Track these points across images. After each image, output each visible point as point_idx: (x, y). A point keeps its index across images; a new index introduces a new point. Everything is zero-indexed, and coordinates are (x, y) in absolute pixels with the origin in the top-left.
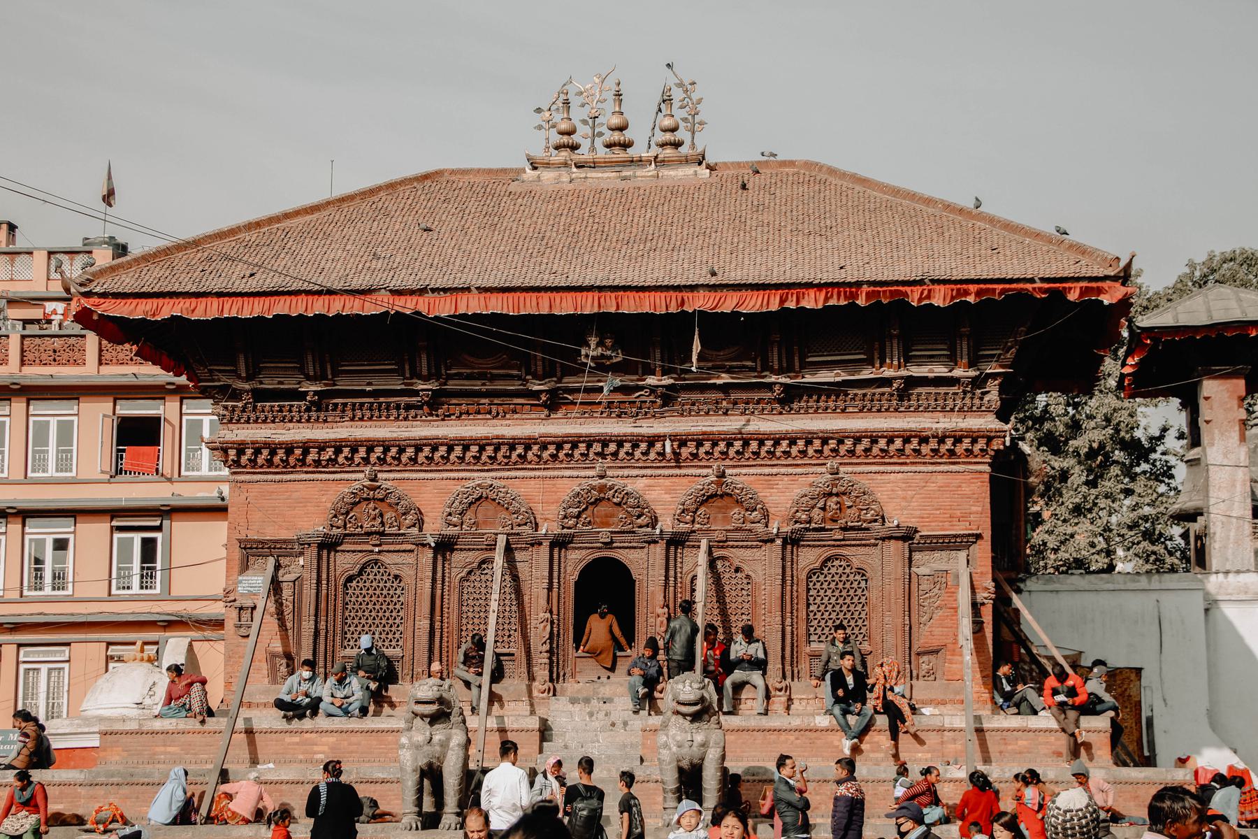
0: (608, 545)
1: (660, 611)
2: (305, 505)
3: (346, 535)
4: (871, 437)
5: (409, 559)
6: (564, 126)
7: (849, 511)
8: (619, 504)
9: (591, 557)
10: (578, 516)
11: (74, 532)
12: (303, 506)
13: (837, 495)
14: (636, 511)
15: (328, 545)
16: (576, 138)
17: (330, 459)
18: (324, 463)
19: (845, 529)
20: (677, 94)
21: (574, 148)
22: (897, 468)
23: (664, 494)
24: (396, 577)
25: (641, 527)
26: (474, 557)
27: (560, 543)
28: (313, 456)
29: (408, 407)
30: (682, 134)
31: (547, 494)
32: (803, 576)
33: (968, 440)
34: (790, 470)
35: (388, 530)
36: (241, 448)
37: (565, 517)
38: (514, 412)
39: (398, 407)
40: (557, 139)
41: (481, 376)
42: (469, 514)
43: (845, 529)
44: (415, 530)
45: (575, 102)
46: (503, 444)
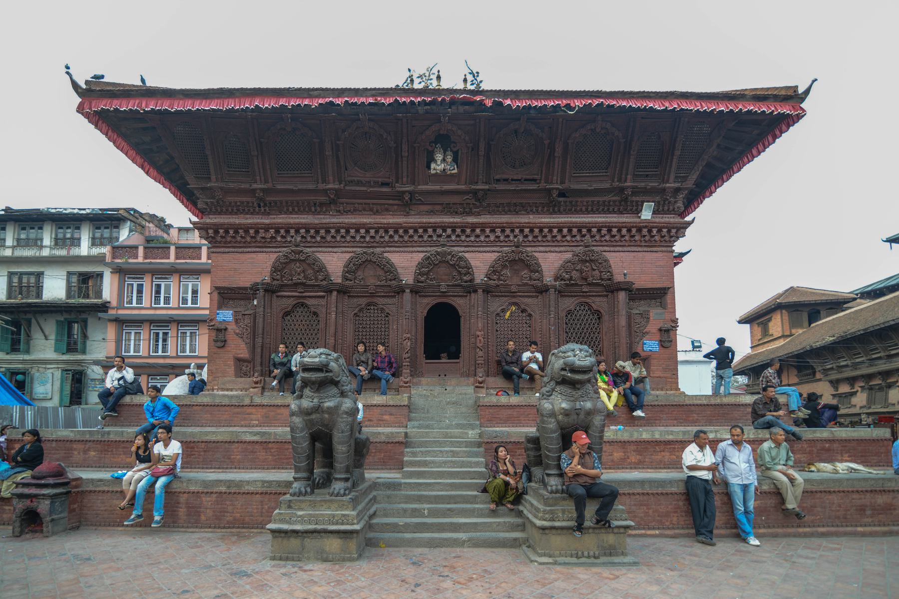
1: (479, 333)
2: (255, 267)
3: (282, 286)
4: (609, 227)
5: (323, 302)
7: (594, 273)
8: (453, 266)
9: (435, 302)
10: (427, 274)
13: (587, 261)
15: (270, 290)
17: (272, 237)
19: (589, 284)
22: (621, 249)
23: (481, 262)
25: (466, 282)
26: (363, 301)
27: (415, 291)
28: (262, 233)
32: (564, 314)
34: (557, 249)
35: (309, 283)
36: (216, 228)
37: (419, 274)
38: (387, 210)
42: (360, 273)
43: (589, 284)
44: (324, 283)
46: (381, 228)
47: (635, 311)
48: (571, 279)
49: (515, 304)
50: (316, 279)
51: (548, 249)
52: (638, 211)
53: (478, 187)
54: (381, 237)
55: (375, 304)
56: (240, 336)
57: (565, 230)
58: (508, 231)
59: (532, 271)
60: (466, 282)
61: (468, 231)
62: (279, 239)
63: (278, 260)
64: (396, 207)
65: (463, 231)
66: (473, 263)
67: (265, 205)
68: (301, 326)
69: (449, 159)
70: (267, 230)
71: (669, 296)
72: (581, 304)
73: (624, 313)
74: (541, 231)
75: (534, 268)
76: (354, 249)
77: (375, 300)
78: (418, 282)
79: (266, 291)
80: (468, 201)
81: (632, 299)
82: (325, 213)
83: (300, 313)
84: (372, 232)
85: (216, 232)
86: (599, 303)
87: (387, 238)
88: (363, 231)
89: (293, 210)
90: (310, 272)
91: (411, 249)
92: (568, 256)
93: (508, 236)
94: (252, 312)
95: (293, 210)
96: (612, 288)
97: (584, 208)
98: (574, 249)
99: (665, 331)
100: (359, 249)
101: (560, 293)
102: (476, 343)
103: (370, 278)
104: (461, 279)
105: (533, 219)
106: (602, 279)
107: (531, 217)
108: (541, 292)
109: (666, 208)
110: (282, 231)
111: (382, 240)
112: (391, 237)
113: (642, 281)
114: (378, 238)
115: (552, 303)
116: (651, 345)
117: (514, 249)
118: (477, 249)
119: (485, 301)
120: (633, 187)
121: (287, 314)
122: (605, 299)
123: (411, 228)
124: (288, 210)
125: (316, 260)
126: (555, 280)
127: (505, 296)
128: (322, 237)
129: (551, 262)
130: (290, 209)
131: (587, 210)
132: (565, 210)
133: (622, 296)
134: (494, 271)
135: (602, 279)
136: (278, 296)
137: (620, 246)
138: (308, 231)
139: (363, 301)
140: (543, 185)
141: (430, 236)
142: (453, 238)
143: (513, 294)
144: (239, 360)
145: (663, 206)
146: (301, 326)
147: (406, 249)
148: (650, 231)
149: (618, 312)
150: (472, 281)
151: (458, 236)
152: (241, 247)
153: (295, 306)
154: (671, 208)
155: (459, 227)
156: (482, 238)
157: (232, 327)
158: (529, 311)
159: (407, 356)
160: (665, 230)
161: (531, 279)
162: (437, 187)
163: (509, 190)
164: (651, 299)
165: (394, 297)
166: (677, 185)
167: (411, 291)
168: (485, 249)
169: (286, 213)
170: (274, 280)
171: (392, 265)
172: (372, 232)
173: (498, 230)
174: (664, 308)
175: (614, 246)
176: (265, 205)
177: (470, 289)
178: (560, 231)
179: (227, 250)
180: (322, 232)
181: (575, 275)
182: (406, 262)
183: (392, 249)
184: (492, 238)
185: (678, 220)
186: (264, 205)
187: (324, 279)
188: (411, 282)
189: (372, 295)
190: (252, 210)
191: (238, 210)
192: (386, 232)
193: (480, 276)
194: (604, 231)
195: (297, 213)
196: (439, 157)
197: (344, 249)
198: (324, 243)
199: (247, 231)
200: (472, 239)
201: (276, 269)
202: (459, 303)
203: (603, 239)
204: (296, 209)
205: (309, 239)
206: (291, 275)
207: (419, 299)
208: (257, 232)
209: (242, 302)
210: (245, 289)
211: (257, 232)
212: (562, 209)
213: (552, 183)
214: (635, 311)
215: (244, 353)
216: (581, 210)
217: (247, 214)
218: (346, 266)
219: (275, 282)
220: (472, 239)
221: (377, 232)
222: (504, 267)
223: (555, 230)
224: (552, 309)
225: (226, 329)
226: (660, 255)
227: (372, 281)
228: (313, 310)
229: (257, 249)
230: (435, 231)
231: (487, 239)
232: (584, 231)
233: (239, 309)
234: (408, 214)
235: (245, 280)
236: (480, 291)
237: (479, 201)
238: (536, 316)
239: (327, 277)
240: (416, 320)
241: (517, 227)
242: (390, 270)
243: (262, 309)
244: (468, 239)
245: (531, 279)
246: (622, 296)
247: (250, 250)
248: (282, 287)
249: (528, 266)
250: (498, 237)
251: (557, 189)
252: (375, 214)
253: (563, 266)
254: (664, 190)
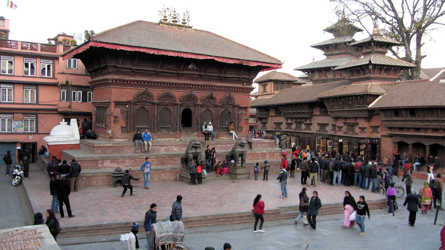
0: (188, 106)
6: (165, 16)
11: (14, 88)
16: (167, 18)
20: (186, 13)
21: (166, 20)
24: (147, 111)
29: (153, 74)
30: (186, 21)
31: (178, 94)
39: (145, 74)
40: (164, 18)
41: (170, 69)
45: (167, 11)
66: (198, 96)
81: (239, 109)
86: (230, 110)
90: (148, 97)
96: (234, 106)
144: (122, 127)
189: (166, 105)
202: (192, 109)
215: (124, 125)
222: (206, 99)
235: (123, 99)
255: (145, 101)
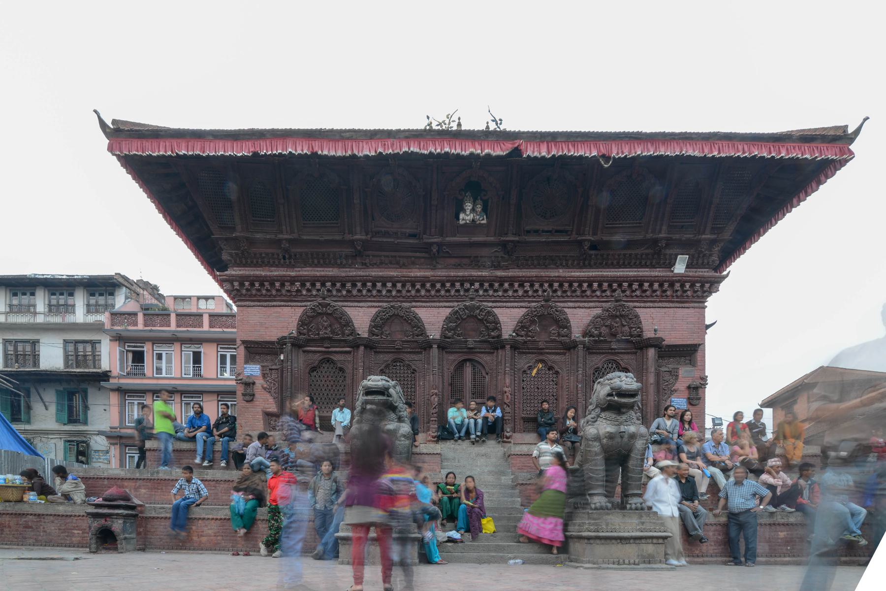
1: (506, 389)
7: (624, 329)
10: (454, 329)
12: (280, 321)
14: (491, 326)
17: (298, 291)
18: (294, 294)
19: (618, 341)
25: (493, 338)
33: (698, 285)
34: (586, 305)
35: (336, 337)
37: (447, 329)
38: (413, 263)
42: (386, 328)
44: (351, 338)
46: (409, 281)
47: (663, 369)
48: (600, 335)
49: (542, 361)
50: (343, 334)
51: (577, 305)
52: (671, 264)
53: (508, 239)
54: (408, 291)
55: (402, 361)
56: (268, 390)
57: (595, 285)
58: (537, 286)
59: (560, 327)
60: (493, 338)
61: (496, 285)
62: (304, 292)
63: (304, 313)
64: (422, 260)
65: (491, 286)
66: (502, 319)
67: (290, 258)
68: (328, 383)
69: (479, 208)
70: (292, 283)
71: (699, 354)
72: (609, 361)
73: (653, 370)
74: (571, 286)
75: (563, 324)
76: (380, 304)
77: (401, 356)
78: (446, 337)
79: (293, 345)
80: (497, 254)
82: (350, 266)
83: (326, 369)
84: (399, 285)
85: (242, 285)
87: (413, 293)
88: (389, 285)
89: (319, 262)
91: (438, 304)
92: (598, 311)
93: (537, 291)
94: (278, 367)
95: (319, 262)
97: (615, 262)
98: (604, 304)
99: (694, 388)
100: (385, 304)
101: (590, 350)
102: (503, 399)
103: (397, 333)
104: (489, 335)
105: (561, 272)
106: (631, 336)
107: (561, 271)
108: (569, 349)
109: (700, 261)
110: (308, 284)
111: (409, 294)
112: (418, 291)
113: (672, 338)
114: (404, 292)
115: (581, 359)
116: (679, 402)
117: (543, 303)
118: (505, 304)
119: (513, 358)
120: (667, 239)
121: (313, 369)
122: (633, 357)
123: (438, 281)
124: (313, 262)
125: (343, 314)
126: (583, 337)
127: (533, 353)
128: (349, 291)
129: (580, 318)
130: (316, 261)
131: (618, 263)
132: (595, 264)
133: (651, 352)
134: (522, 326)
135: (631, 336)
136: (304, 352)
137: (651, 302)
138: (334, 285)
139: (389, 357)
140: (574, 236)
141: (458, 291)
142: (481, 292)
143: (540, 351)
145: (697, 260)
146: (328, 383)
147: (433, 304)
148: (682, 286)
149: (647, 369)
150: (500, 336)
151: (486, 291)
152: (266, 301)
153: (321, 362)
154: (706, 261)
155: (487, 281)
156: (510, 293)
157: (260, 382)
158: (556, 368)
159: (434, 411)
160: (698, 285)
161: (559, 335)
162: (466, 239)
163: (540, 242)
164: (680, 357)
165: (421, 353)
166: (713, 237)
167: (438, 347)
168: (512, 304)
169: (311, 266)
170: (301, 334)
171: (419, 320)
172: (399, 285)
173: (527, 285)
174: (694, 366)
175: (645, 302)
176: (290, 258)
177: (497, 345)
178: (590, 285)
179: (252, 304)
180: (349, 285)
181: (604, 330)
182: (433, 318)
183: (418, 304)
184: (520, 293)
185: (712, 274)
186: (289, 259)
187: (351, 334)
188: (438, 337)
190: (277, 263)
191: (263, 262)
192: (413, 286)
193: (507, 331)
194: (635, 286)
195: (322, 266)
196: (469, 206)
197: (370, 304)
198: (349, 298)
199: (272, 284)
200: (500, 293)
201: (303, 323)
203: (634, 294)
204: (322, 262)
205: (334, 293)
206: (319, 329)
207: (445, 355)
208: (282, 285)
209: (269, 357)
210: (272, 343)
211: (282, 285)
212: (592, 263)
213: (583, 234)
214: (663, 369)
215: (273, 408)
216: (612, 264)
217: (272, 266)
218: (373, 321)
219: (302, 337)
220: (500, 293)
221: (403, 286)
222: (533, 322)
223: (585, 285)
224: (581, 365)
225: (254, 383)
226: (691, 311)
227: (399, 337)
228: (339, 365)
229: (282, 303)
230: (462, 285)
231: (515, 294)
232: (615, 285)
233: (266, 364)
234: (434, 268)
236: (508, 347)
237: (510, 253)
238: (564, 373)
239: (353, 332)
240: (443, 376)
241: (546, 282)
242: (417, 325)
243: (289, 363)
244: (496, 294)
245: (559, 335)
246: (651, 352)
247: (275, 303)
248: (309, 342)
249: (557, 322)
250: (526, 292)
251: (590, 240)
252: (401, 268)
253: (592, 322)
254: (699, 241)
255: (329, 339)
